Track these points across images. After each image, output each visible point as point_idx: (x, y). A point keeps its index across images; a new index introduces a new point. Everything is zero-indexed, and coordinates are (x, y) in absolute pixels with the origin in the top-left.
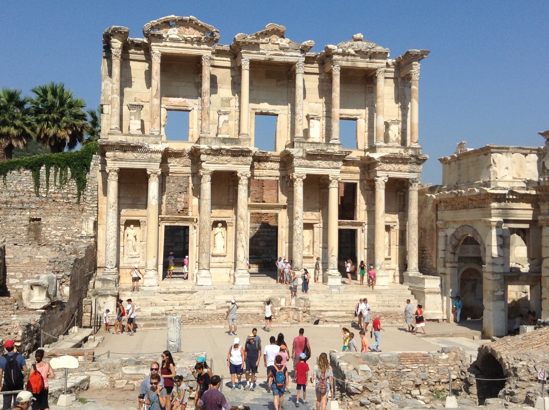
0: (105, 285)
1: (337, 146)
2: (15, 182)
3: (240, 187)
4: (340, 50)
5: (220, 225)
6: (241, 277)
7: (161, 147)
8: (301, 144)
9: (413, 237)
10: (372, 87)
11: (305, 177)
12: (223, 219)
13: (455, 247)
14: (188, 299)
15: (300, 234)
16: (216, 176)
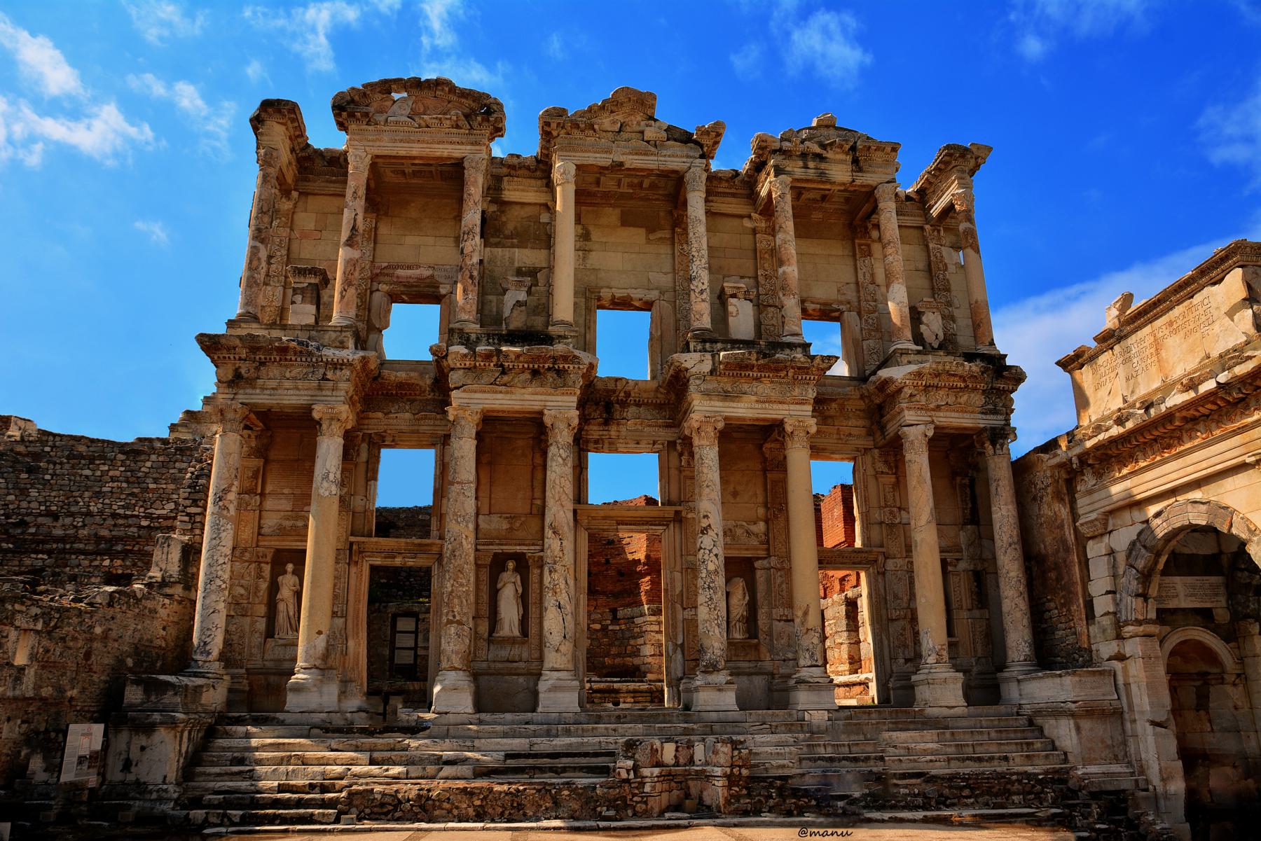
0: (153, 698)
1: (799, 350)
2: (87, 494)
3: (552, 450)
4: (786, 145)
5: (511, 565)
6: (555, 689)
7: (350, 354)
8: (708, 345)
9: (1012, 574)
10: (869, 246)
11: (720, 425)
12: (518, 549)
13: (1145, 577)
14: (398, 746)
15: (716, 572)
16: (493, 429)
